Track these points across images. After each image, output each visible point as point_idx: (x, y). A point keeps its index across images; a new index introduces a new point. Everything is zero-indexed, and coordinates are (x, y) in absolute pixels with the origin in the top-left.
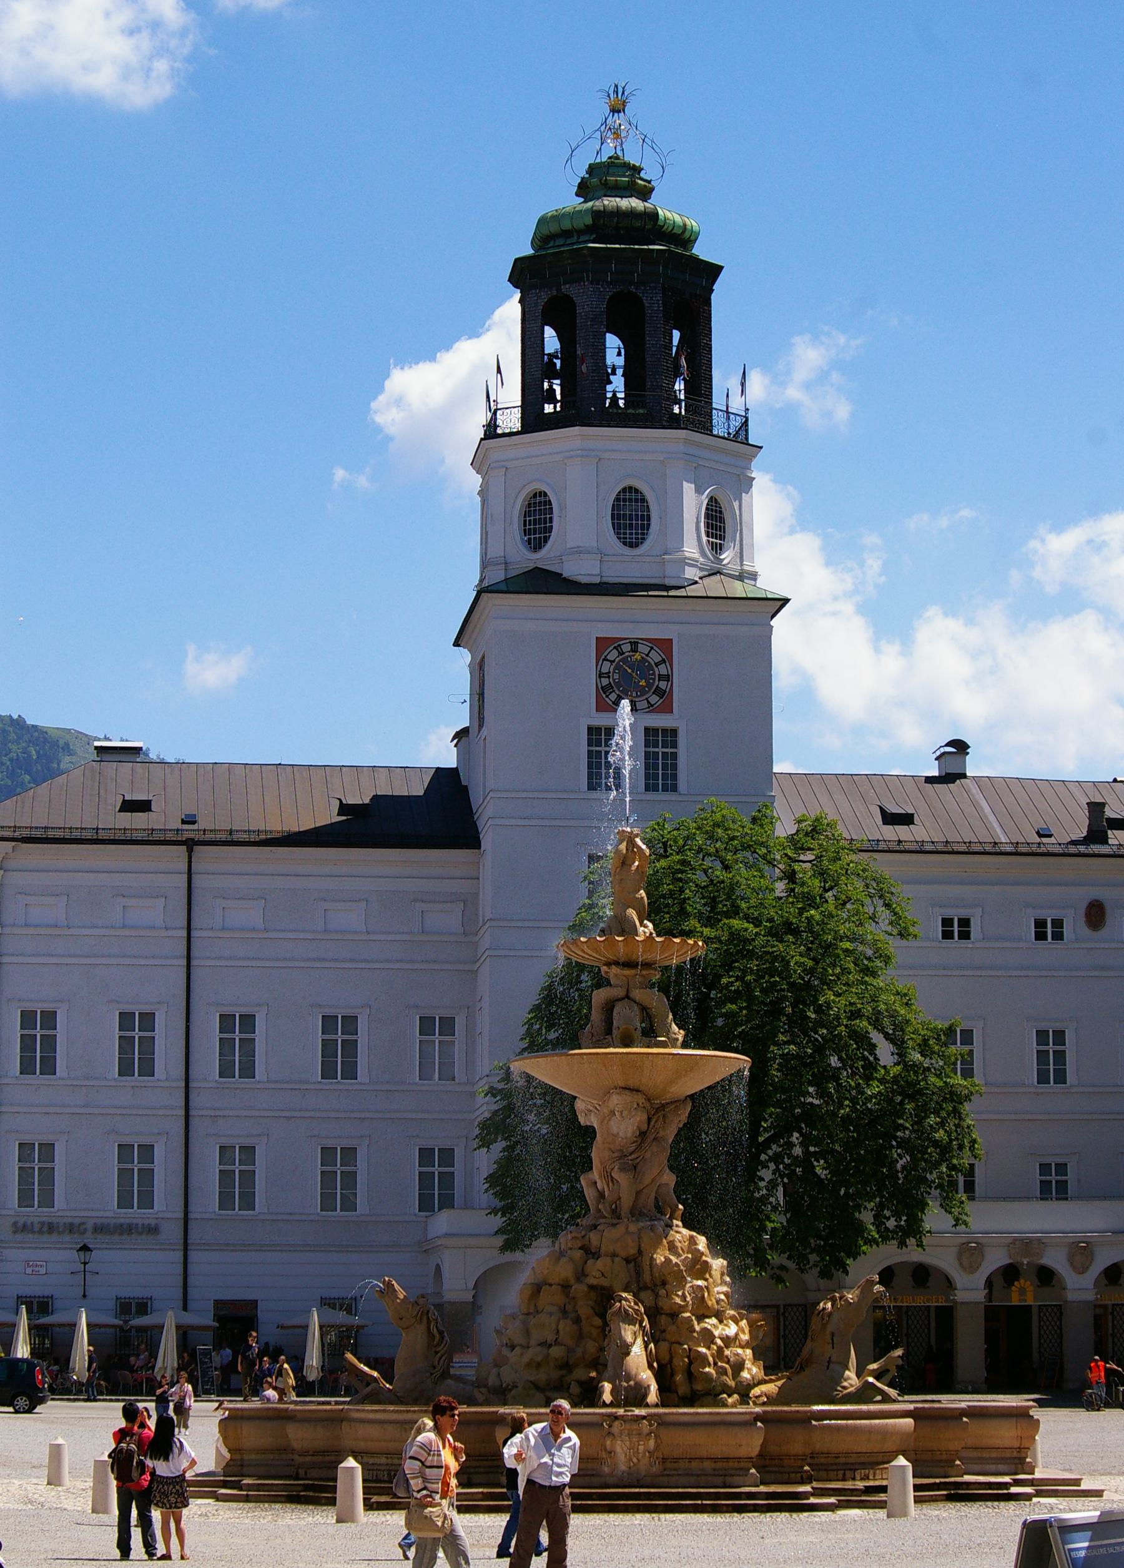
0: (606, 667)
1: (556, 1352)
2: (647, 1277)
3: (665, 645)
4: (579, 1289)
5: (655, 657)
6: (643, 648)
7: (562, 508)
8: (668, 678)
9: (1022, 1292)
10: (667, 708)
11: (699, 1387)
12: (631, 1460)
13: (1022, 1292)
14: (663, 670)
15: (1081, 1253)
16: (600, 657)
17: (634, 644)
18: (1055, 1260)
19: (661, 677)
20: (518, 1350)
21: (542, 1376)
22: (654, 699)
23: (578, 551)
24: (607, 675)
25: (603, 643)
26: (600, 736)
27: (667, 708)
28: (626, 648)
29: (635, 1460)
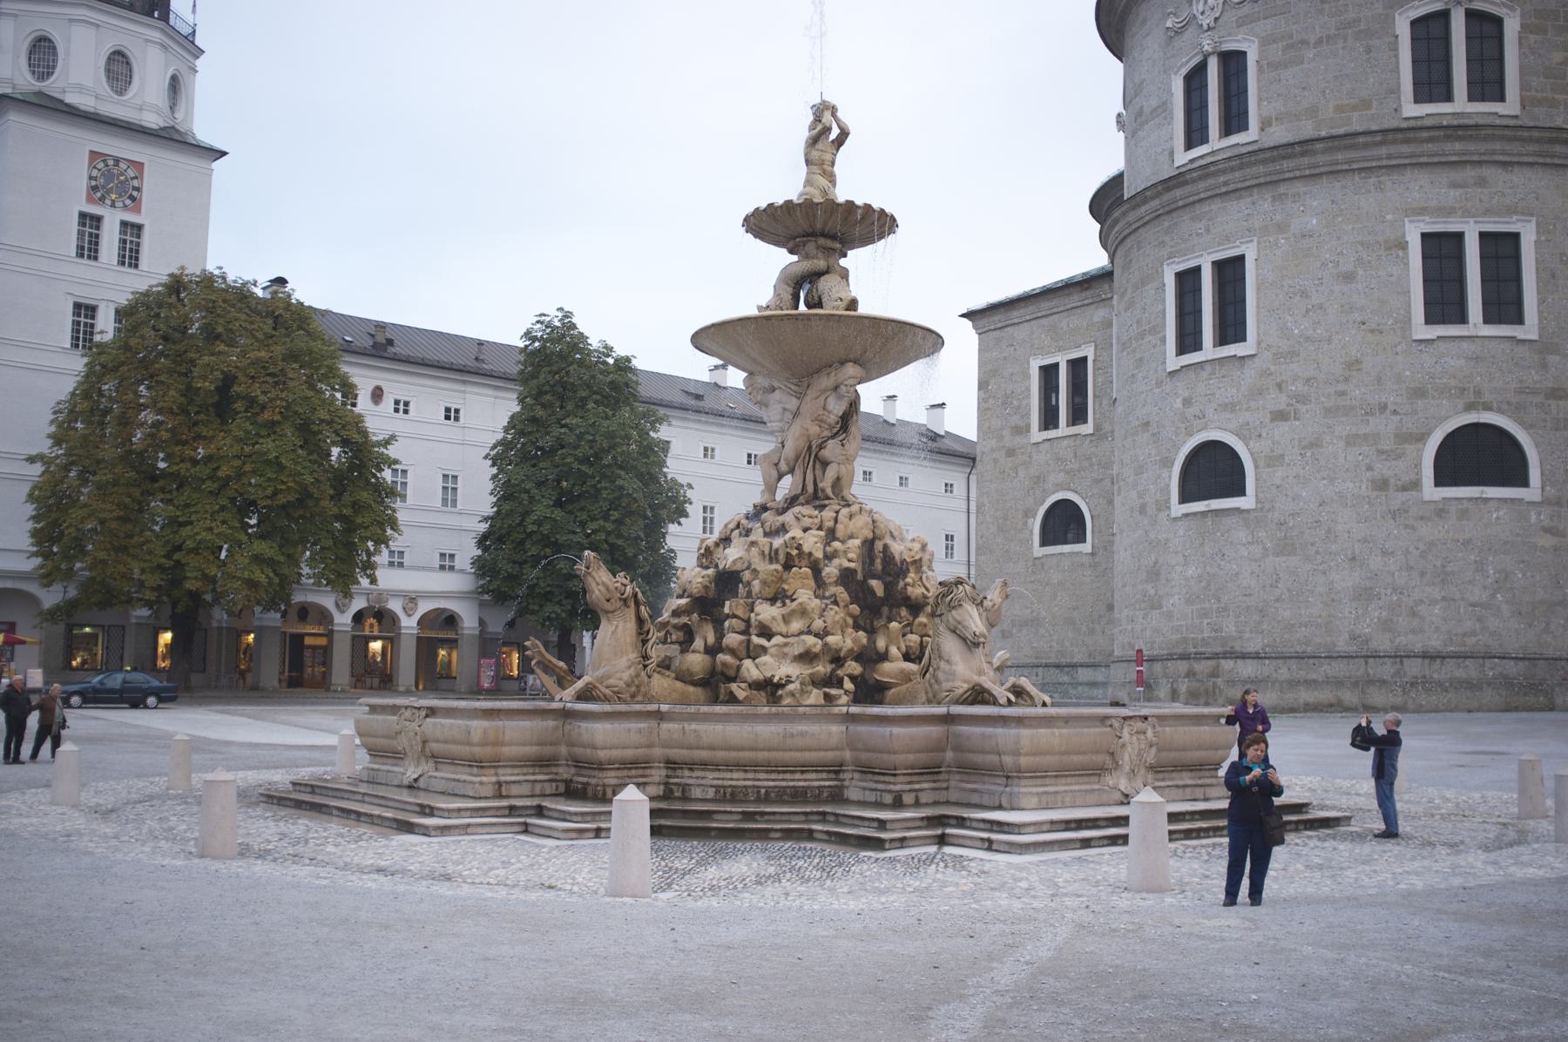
0: (95, 173)
3: (139, 166)
4: (831, 571)
5: (131, 173)
6: (123, 166)
7: (67, 53)
8: (138, 189)
9: (372, 626)
13: (372, 626)
14: (135, 183)
15: (411, 600)
16: (92, 166)
17: (117, 161)
18: (395, 606)
19: (135, 189)
20: (777, 640)
21: (822, 668)
22: (128, 202)
23: (80, 88)
24: (95, 179)
26: (90, 221)
27: (138, 210)
28: (111, 162)
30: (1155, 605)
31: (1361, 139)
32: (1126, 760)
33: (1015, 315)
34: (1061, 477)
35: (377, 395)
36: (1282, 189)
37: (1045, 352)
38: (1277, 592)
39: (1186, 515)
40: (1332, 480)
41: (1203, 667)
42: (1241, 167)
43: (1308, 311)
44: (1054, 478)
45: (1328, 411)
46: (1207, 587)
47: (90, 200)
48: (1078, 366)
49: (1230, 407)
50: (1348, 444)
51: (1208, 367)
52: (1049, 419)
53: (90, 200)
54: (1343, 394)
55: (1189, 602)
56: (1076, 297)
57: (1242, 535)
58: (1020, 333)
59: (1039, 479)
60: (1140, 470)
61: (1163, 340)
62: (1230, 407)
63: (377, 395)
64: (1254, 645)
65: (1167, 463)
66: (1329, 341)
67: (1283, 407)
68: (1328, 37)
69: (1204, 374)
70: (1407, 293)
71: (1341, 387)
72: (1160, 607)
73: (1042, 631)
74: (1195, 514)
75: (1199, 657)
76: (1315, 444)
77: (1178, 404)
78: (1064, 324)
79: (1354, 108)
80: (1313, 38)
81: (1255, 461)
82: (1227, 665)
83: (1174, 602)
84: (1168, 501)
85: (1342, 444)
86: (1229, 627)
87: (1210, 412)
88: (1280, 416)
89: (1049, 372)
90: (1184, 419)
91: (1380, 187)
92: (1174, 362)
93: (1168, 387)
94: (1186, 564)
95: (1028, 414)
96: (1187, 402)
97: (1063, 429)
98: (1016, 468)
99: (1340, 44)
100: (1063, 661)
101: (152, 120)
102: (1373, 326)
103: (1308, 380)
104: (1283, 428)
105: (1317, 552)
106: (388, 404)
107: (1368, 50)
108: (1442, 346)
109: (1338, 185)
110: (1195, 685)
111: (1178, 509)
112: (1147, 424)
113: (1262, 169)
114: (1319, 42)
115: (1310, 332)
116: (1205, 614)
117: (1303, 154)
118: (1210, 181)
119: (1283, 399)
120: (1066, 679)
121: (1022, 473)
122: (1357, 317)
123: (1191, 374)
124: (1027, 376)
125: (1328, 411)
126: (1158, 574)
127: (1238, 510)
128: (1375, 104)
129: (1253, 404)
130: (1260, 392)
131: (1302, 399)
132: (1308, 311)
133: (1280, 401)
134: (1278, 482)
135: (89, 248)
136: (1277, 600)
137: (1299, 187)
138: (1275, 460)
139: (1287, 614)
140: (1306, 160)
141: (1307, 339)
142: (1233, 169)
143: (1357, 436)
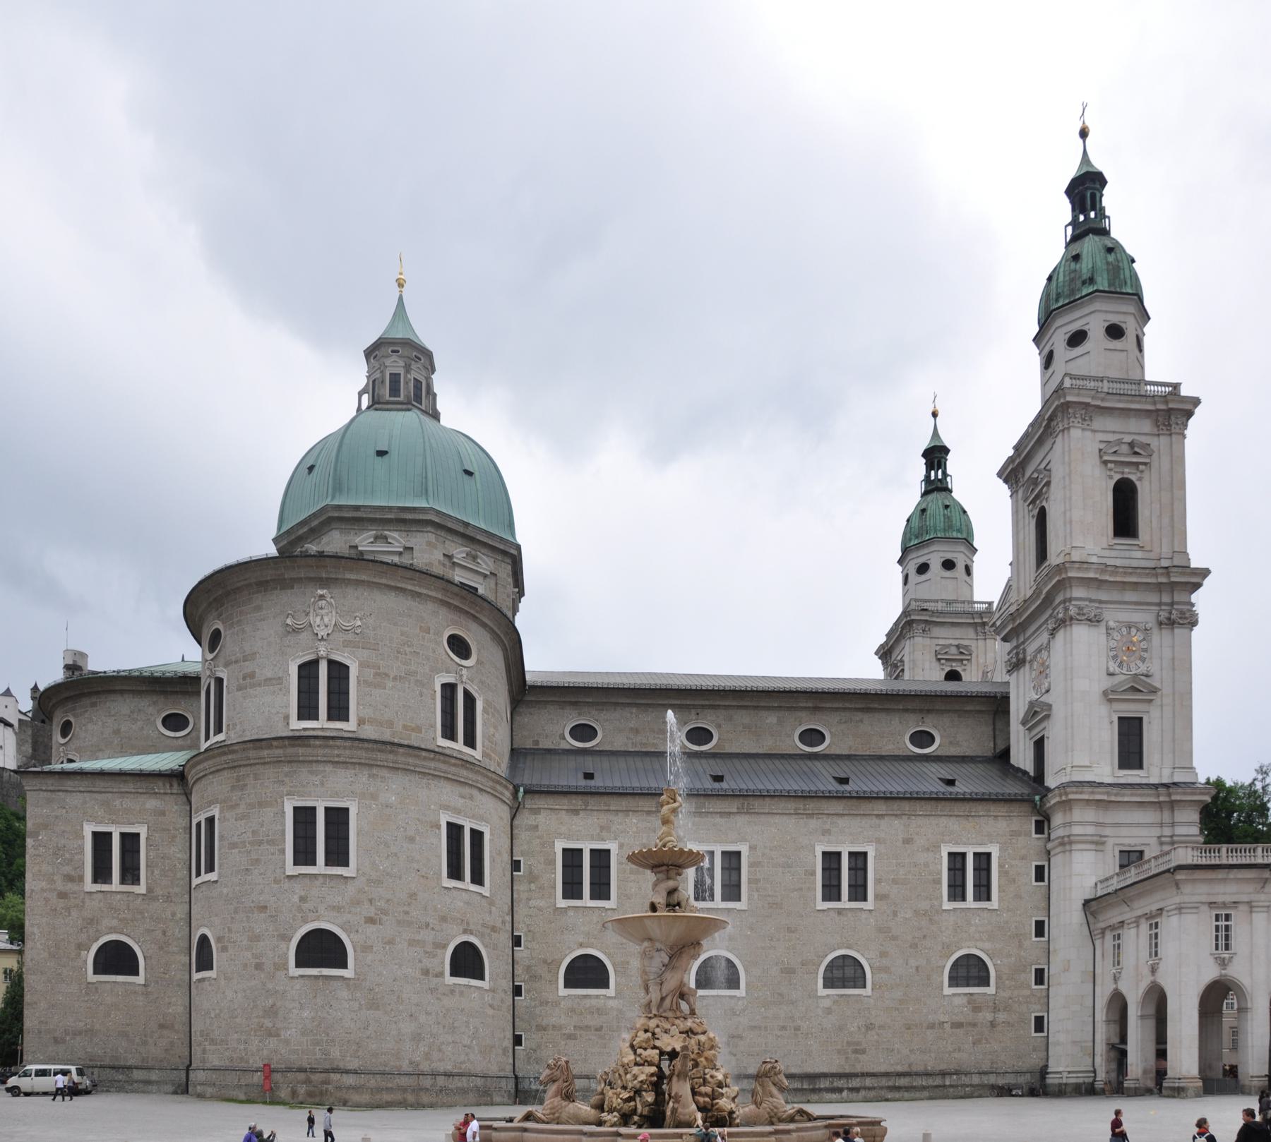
33: (69, 784)
45: (399, 922)
49: (337, 909)
51: (321, 880)
54: (407, 913)
56: (131, 785)
58: (74, 800)
62: (337, 909)
69: (318, 883)
70: (440, 857)
71: (406, 908)
77: (296, 899)
78: (117, 802)
81: (354, 947)
87: (322, 909)
88: (371, 921)
90: (300, 909)
92: (291, 869)
93: (286, 885)
94: (302, 1007)
96: (303, 899)
104: (371, 929)
108: (455, 893)
112: (266, 907)
119: (373, 909)
122: (415, 866)
123: (307, 881)
125: (399, 922)
130: (358, 903)
131: (385, 913)
133: (371, 912)
141: (388, 874)
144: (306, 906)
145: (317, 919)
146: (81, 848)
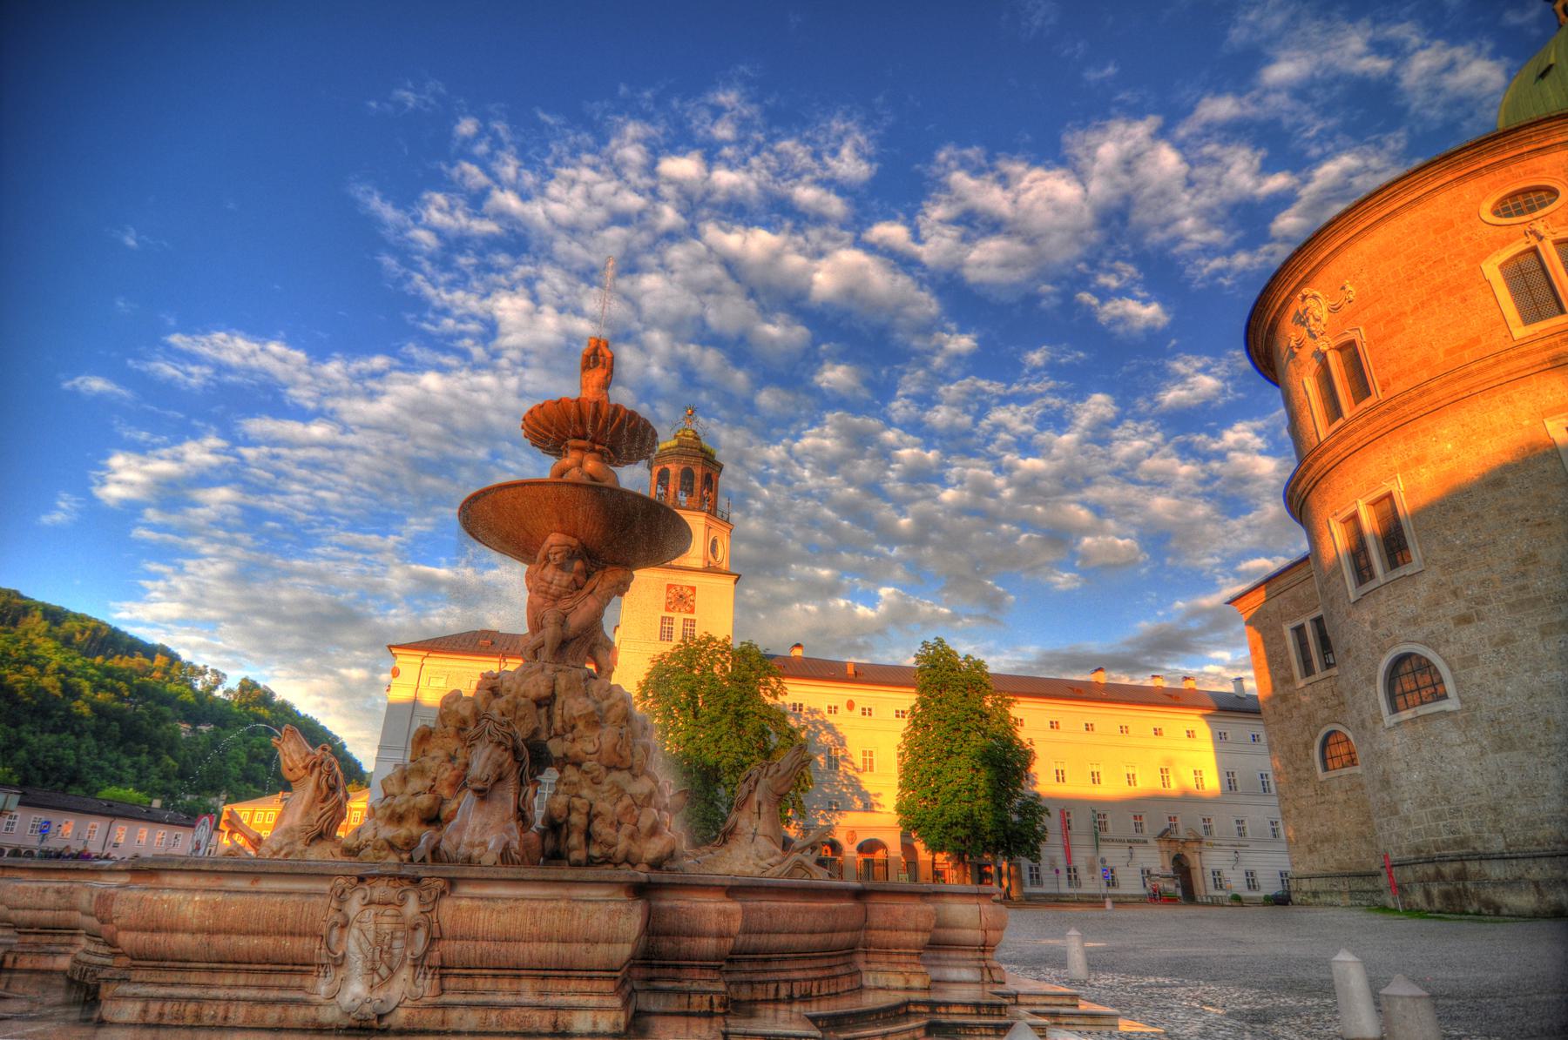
1: (425, 801)
2: (558, 724)
3: (693, 589)
10: (692, 611)
11: (595, 851)
12: (374, 970)
25: (670, 586)
27: (692, 611)
29: (384, 971)
30: (1395, 812)
31: (1474, 367)
32: (354, 945)
34: (1326, 713)
35: (851, 705)
36: (1410, 429)
37: (1291, 617)
38: (1507, 790)
39: (1398, 724)
40: (1537, 671)
41: (1447, 869)
42: (1369, 422)
43: (1464, 522)
44: (1323, 714)
46: (1434, 790)
47: (667, 609)
48: (1318, 622)
49: (1414, 621)
50: (1543, 634)
51: (1385, 592)
52: (1308, 669)
53: (667, 609)
54: (1524, 588)
55: (1423, 806)
57: (1454, 736)
59: (1309, 718)
60: (1354, 691)
61: (1343, 578)
63: (851, 705)
64: (1498, 845)
65: (1371, 680)
66: (1494, 543)
67: (1464, 611)
68: (1423, 304)
69: (1383, 598)
71: (1518, 582)
72: (1397, 813)
73: (1340, 845)
74: (1406, 722)
75: (1443, 859)
76: (1507, 640)
77: (1368, 628)
79: (1464, 347)
80: (1408, 309)
82: (1473, 867)
83: (1406, 807)
84: (1380, 714)
85: (1536, 636)
86: (1466, 827)
88: (1464, 620)
89: (1300, 631)
91: (1508, 401)
95: (1290, 667)
96: (1374, 624)
97: (1319, 673)
98: (1289, 710)
99: (1435, 303)
100: (1363, 870)
101: (699, 564)
102: (1538, 520)
103: (1483, 582)
104: (1467, 633)
105: (1540, 745)
106: (858, 711)
107: (1464, 300)
109: (1464, 411)
110: (1444, 887)
111: (1389, 719)
113: (1386, 418)
114: (1416, 309)
115: (1472, 540)
116: (1438, 817)
117: (1421, 395)
118: (1347, 442)
120: (1368, 887)
121: (1295, 713)
122: (1519, 516)
124: (1282, 638)
126: (1388, 782)
127: (1446, 713)
128: (1483, 338)
129: (1433, 614)
131: (1483, 601)
132: (1464, 522)
133: (1461, 607)
134: (1477, 680)
135: (666, 635)
136: (1509, 797)
137: (1427, 422)
138: (1470, 661)
139: (1524, 810)
140: (1425, 399)
141: (1471, 546)
142: (1362, 426)
143: (1551, 624)
144: (1380, 631)
145: (1395, 644)
146: (1286, 647)
